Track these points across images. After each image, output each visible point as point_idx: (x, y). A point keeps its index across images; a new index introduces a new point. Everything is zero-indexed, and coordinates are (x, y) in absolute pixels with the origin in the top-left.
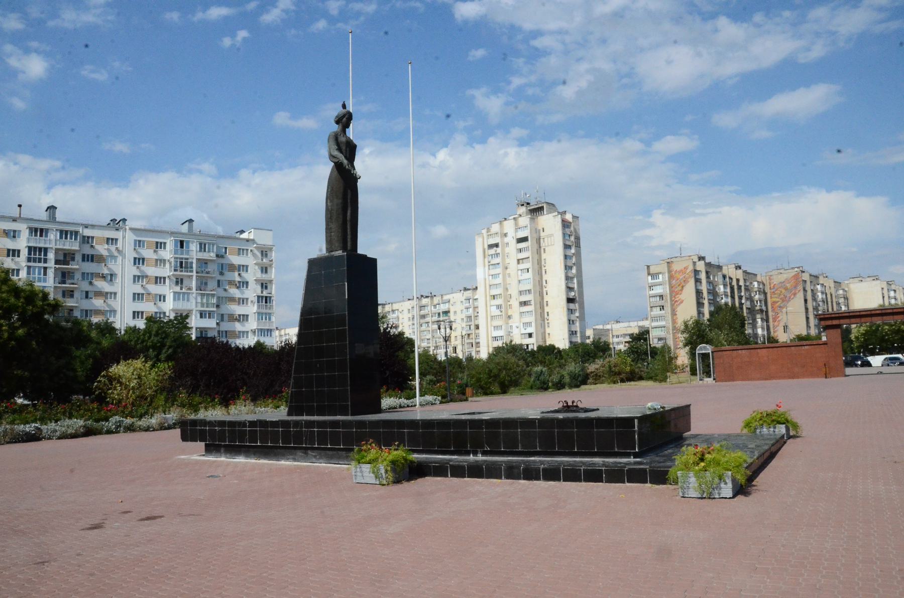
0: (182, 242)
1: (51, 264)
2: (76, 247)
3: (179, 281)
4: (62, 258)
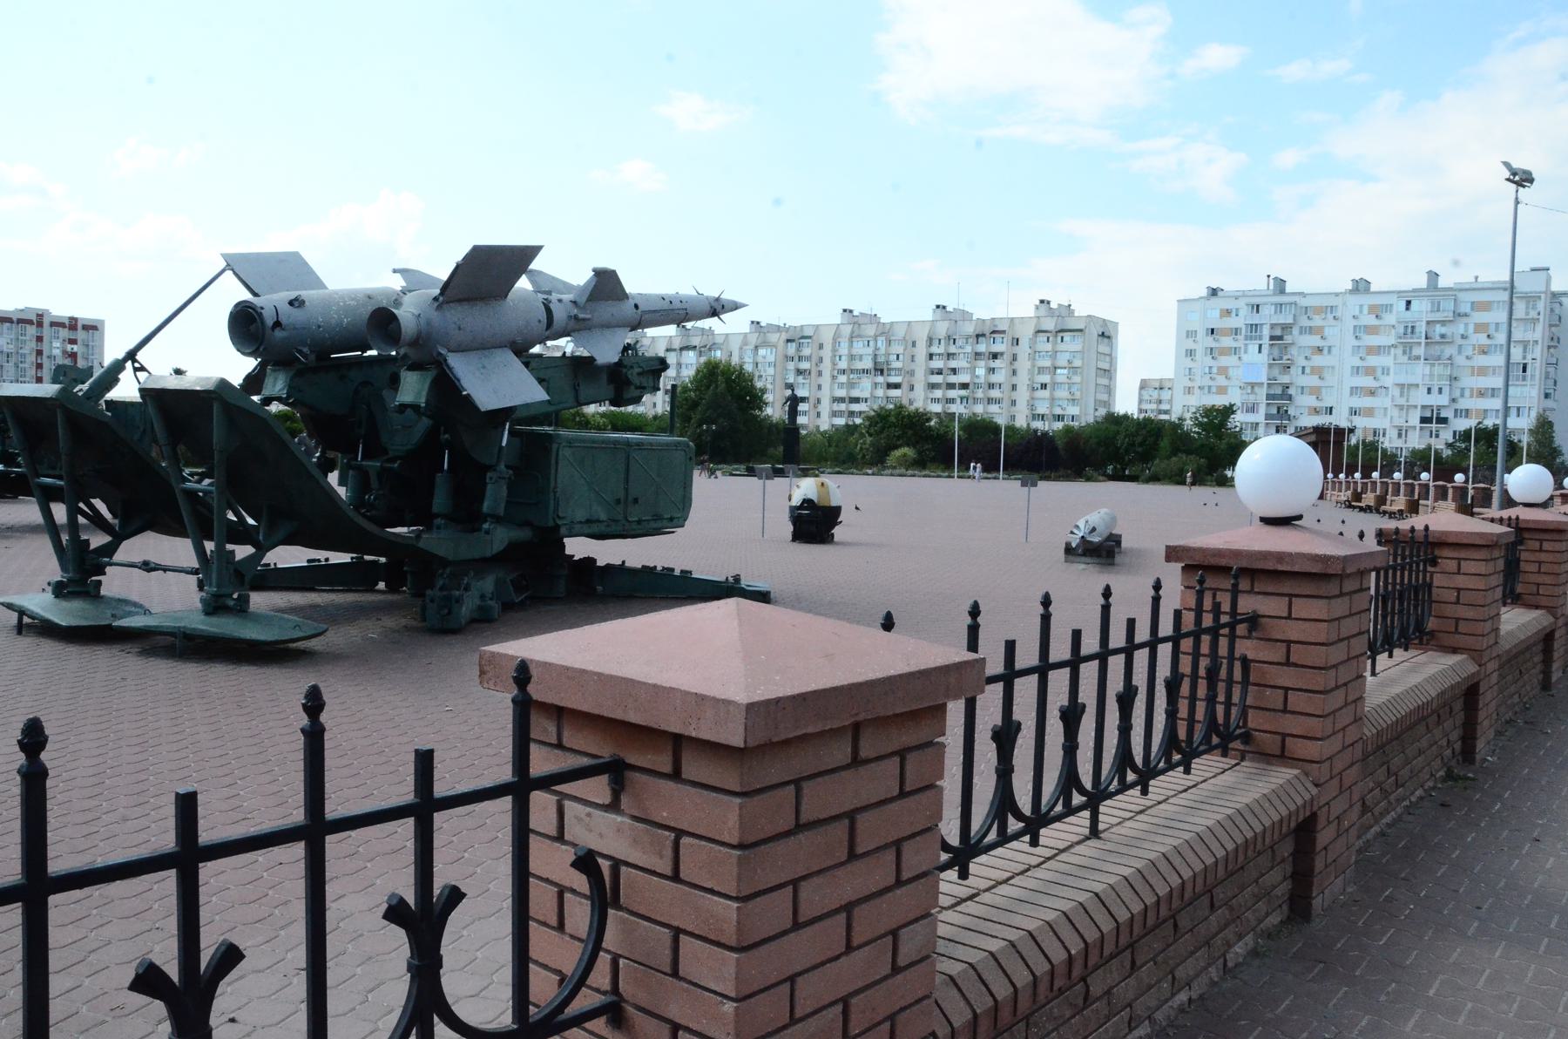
0: (1409, 303)
1: (1266, 341)
2: (1290, 320)
3: (1407, 348)
4: (1278, 332)
